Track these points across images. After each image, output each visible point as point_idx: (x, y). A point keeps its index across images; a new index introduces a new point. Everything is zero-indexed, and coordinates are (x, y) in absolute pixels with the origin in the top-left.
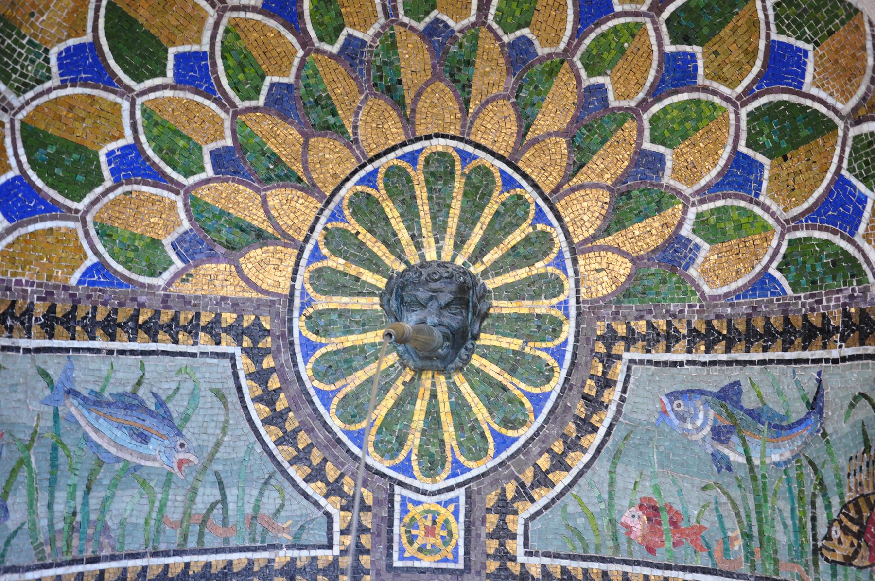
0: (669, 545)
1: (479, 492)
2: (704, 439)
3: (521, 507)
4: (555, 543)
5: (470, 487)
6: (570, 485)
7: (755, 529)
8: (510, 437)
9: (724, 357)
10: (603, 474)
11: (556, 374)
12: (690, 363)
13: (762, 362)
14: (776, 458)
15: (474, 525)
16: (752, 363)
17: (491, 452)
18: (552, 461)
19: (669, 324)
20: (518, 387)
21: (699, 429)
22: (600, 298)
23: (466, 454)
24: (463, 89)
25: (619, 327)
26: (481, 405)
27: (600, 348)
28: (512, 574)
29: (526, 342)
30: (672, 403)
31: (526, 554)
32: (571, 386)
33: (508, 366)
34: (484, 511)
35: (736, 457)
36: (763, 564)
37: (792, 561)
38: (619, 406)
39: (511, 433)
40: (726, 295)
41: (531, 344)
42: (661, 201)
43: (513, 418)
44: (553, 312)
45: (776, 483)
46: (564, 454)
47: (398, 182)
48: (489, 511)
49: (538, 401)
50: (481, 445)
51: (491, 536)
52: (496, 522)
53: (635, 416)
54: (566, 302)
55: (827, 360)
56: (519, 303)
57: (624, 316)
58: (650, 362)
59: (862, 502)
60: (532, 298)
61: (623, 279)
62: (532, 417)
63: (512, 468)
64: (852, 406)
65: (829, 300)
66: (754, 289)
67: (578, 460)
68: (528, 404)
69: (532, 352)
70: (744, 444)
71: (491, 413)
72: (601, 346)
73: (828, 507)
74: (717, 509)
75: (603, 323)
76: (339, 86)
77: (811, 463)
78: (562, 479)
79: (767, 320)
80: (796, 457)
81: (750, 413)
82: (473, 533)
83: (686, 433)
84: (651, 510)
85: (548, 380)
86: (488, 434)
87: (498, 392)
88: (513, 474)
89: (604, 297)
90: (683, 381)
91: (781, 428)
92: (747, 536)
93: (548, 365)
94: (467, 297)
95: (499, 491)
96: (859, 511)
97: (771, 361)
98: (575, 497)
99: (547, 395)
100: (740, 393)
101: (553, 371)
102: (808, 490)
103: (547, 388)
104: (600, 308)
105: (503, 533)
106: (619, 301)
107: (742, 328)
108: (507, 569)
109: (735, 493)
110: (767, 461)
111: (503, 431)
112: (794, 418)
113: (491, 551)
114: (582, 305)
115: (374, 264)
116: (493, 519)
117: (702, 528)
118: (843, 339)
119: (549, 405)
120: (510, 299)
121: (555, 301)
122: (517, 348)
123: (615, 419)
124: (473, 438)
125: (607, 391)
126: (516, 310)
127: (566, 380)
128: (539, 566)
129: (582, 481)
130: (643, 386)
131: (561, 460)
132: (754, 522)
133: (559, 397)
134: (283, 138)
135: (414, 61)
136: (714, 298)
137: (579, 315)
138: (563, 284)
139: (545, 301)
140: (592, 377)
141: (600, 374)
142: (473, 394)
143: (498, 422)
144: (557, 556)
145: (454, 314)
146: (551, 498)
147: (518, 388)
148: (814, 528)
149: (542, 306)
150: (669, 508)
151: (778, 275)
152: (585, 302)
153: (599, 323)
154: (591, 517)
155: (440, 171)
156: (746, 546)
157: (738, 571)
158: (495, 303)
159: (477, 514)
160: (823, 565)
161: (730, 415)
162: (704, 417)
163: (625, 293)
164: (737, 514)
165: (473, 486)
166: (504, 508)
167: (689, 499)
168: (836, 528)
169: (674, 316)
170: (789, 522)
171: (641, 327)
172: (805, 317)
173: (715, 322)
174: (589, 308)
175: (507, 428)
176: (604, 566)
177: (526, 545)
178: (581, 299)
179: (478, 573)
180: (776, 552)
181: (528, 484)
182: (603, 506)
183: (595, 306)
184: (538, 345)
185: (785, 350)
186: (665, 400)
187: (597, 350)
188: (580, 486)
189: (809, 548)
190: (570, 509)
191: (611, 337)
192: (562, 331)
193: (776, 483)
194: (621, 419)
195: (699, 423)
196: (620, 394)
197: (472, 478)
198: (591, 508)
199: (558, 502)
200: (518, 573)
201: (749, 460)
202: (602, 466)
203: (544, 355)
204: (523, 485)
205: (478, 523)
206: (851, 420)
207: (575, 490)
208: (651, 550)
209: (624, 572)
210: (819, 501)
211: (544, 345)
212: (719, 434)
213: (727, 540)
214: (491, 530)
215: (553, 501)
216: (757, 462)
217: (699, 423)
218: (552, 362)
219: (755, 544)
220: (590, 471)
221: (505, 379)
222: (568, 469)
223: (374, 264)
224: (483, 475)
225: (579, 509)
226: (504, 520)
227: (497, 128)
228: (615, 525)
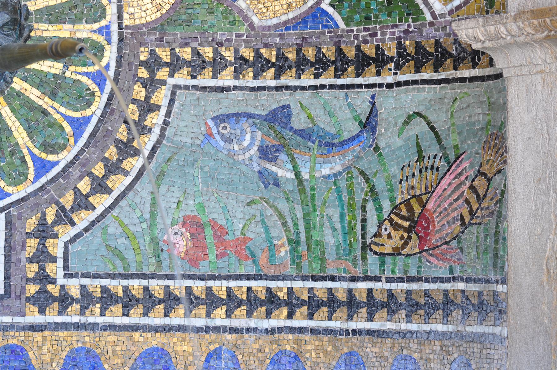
0: (212, 257)
1: (19, 217)
2: (250, 159)
3: (61, 231)
4: (95, 263)
5: (10, 212)
6: (111, 208)
7: (303, 236)
8: (50, 162)
9: (273, 83)
10: (145, 196)
11: (97, 99)
12: (235, 88)
13: (315, 88)
14: (326, 171)
15: (14, 250)
16: (304, 88)
17: (31, 176)
18: (92, 185)
19: (216, 52)
20: (58, 111)
21: (249, 148)
22: (144, 25)
23: (7, 179)
25: (164, 53)
26: (21, 129)
27: (143, 73)
28: (52, 296)
29: (66, 66)
30: (217, 126)
31: (65, 276)
32: (113, 110)
33: (48, 90)
34: (24, 235)
35: (284, 173)
36: (310, 265)
37: (339, 258)
38: (163, 130)
39: (51, 158)
40: (276, 26)
41: (72, 68)
43: (53, 142)
44: (95, 37)
45: (326, 193)
46: (105, 177)
48: (29, 235)
49: (78, 125)
50: (21, 169)
51: (30, 260)
52: (36, 246)
53: (177, 139)
54: (108, 27)
55: (381, 85)
56: (60, 26)
57: (169, 43)
58: (195, 87)
59: (413, 202)
60: (73, 22)
61: (168, 7)
62: (72, 140)
63: (52, 192)
64: (406, 123)
65: (383, 34)
66: (305, 22)
67: (118, 183)
68: (68, 129)
69: (74, 77)
70: (293, 160)
71: (31, 138)
73: (379, 209)
74: (263, 221)
75: (146, 49)
77: (362, 173)
78: (102, 202)
79: (319, 50)
80: (348, 170)
81: (301, 133)
82: (13, 259)
83: (231, 155)
84: (194, 225)
85: (89, 104)
86: (28, 159)
87: (40, 116)
88: (53, 198)
89: (148, 23)
90: (229, 106)
91: (331, 145)
92: (294, 243)
93: (88, 89)
95: (39, 215)
96: (410, 209)
97: (323, 87)
98: (117, 219)
99: (87, 120)
100: (290, 115)
101: (94, 95)
102: (359, 197)
103: (88, 112)
104: (143, 34)
105: (43, 256)
106: (162, 29)
107: (292, 56)
108: (46, 292)
109: (283, 205)
110: (317, 175)
111: (43, 155)
112: (346, 136)
113: (31, 275)
114: (123, 30)
116: (33, 243)
117: (246, 240)
118: (398, 67)
119: (89, 129)
120: (51, 23)
121: (96, 26)
122: (57, 72)
123: (159, 142)
124: (13, 163)
125: (152, 115)
126: (57, 34)
127: (108, 104)
128: (79, 287)
129: (123, 203)
130: (184, 110)
131: (102, 183)
132: (302, 229)
133: (99, 121)
136: (264, 28)
137: (121, 40)
138: (105, 10)
139: (86, 25)
140: (134, 101)
141: (143, 99)
142: (13, 118)
143: (38, 146)
144: (97, 276)
145: (7, 35)
146: (91, 220)
147: (58, 113)
148: (363, 228)
150: (213, 223)
151: (330, 10)
152: (128, 27)
153: (142, 49)
154: (130, 236)
156: (294, 250)
157: (284, 273)
158: (36, 25)
159: (17, 239)
160: (371, 258)
161: (278, 135)
162: (251, 139)
164: (284, 224)
165: (14, 211)
166: (44, 232)
167: (235, 214)
168: (387, 224)
169: (220, 44)
170: (338, 226)
171: (186, 53)
172: (358, 48)
173: (263, 51)
174: (132, 33)
175: (47, 152)
176: (145, 283)
177: (65, 267)
178: (124, 25)
179: (19, 297)
180: (323, 253)
181: (68, 207)
182: (144, 225)
183: (137, 30)
184: (79, 69)
185: (337, 76)
186: (211, 123)
187: (140, 75)
188: (121, 207)
189: (358, 246)
190: (111, 230)
191: (154, 63)
192: (103, 55)
193: (326, 193)
194: (164, 142)
195: (246, 144)
196: (163, 118)
197: (12, 203)
198: (132, 228)
199: (98, 224)
200: (57, 295)
201: (298, 174)
202: (144, 189)
203: (84, 79)
204: (63, 209)
205: (18, 248)
206: (405, 135)
207: (116, 212)
208: (194, 263)
209: (165, 286)
210: (370, 206)
211: (85, 69)
212: (266, 153)
213: (272, 248)
214: (31, 254)
215: (93, 223)
216: (306, 176)
217: (246, 144)
218: (93, 86)
219: (303, 249)
220: (131, 194)
221: (46, 103)
222: (109, 191)
224: (23, 199)
225: (120, 230)
226: (44, 244)
228: (157, 244)
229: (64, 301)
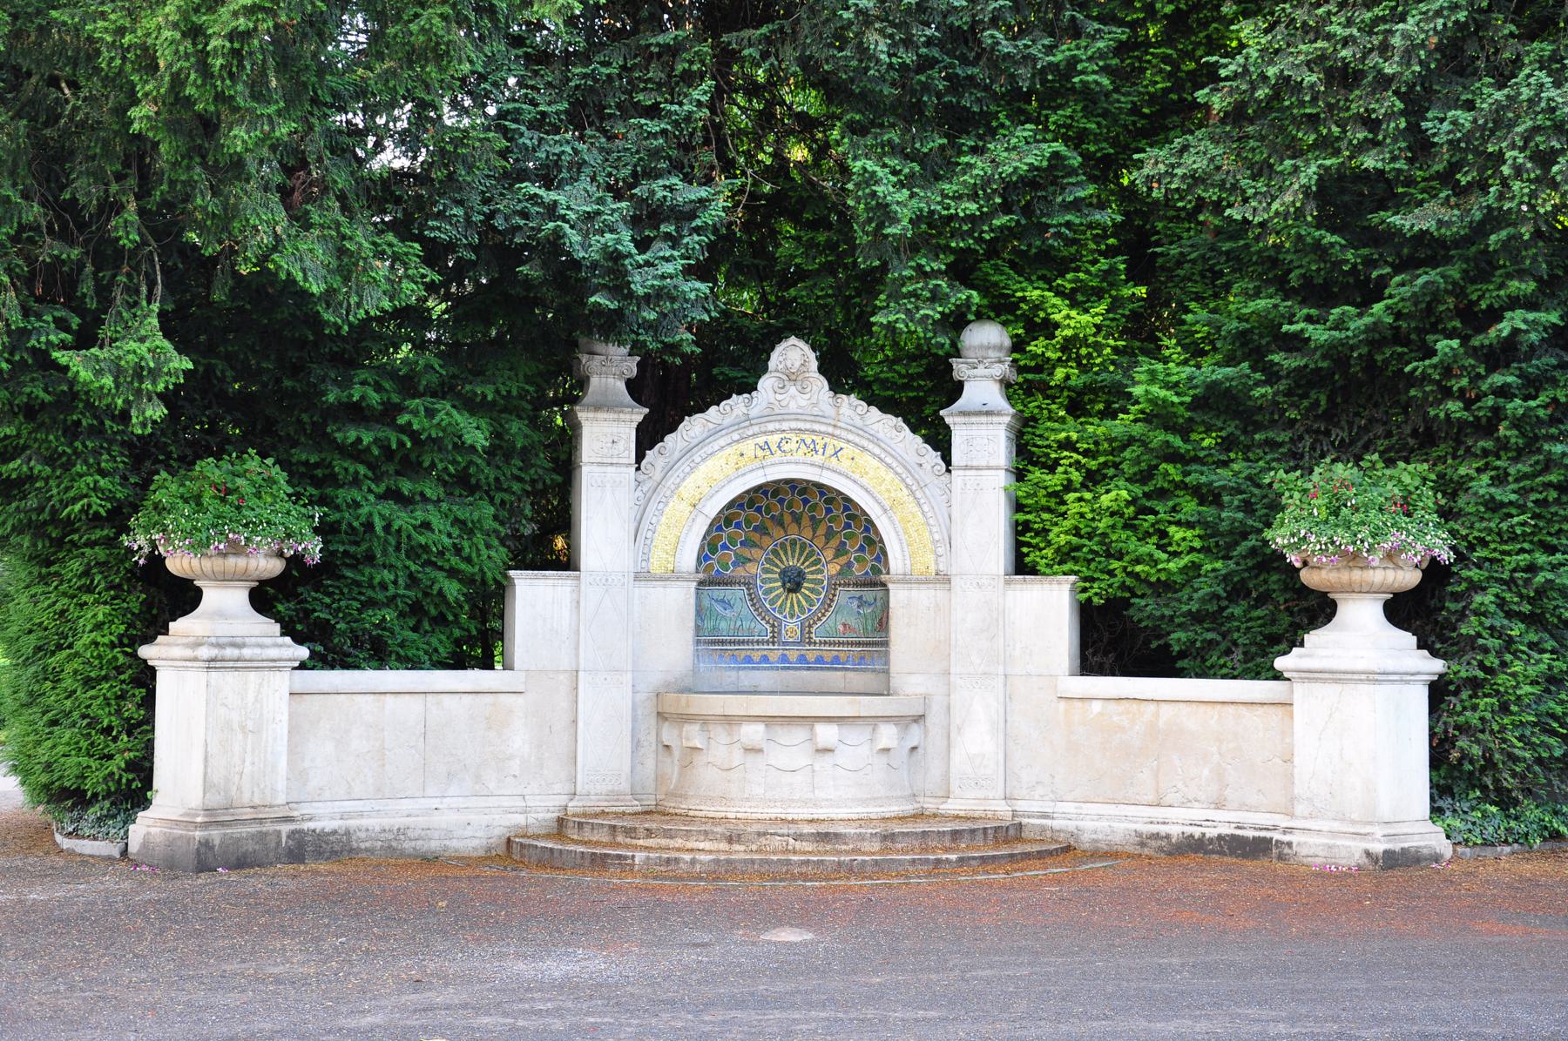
24: (799, 525)
42: (847, 552)
47: (783, 546)
72: (833, 587)
76: (769, 524)
94: (801, 574)
130: (843, 595)
134: (756, 537)
135: (787, 519)
155: (793, 543)
162: (856, 603)
166: (810, 626)
167: (852, 622)
227: (808, 533)
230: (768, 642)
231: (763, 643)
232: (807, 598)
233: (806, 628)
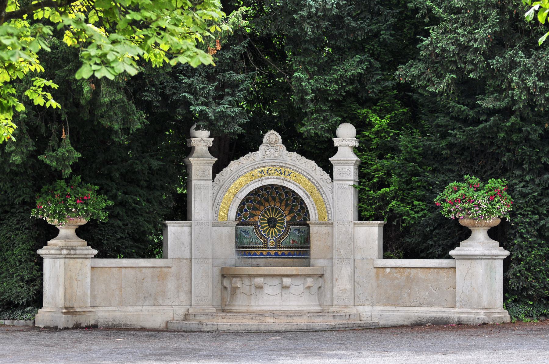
20: (280, 229)
47: (268, 210)
84: (293, 240)
91: (303, 232)
105: (279, 243)
115: (266, 217)
130: (292, 229)
134: (258, 206)
149: (283, 221)
155: (272, 208)
162: (297, 232)
163: (290, 220)
166: (279, 241)
167: (296, 239)
223: (266, 217)
229: (281, 248)
230: (263, 247)
231: (261, 247)
232: (278, 230)
233: (278, 241)
